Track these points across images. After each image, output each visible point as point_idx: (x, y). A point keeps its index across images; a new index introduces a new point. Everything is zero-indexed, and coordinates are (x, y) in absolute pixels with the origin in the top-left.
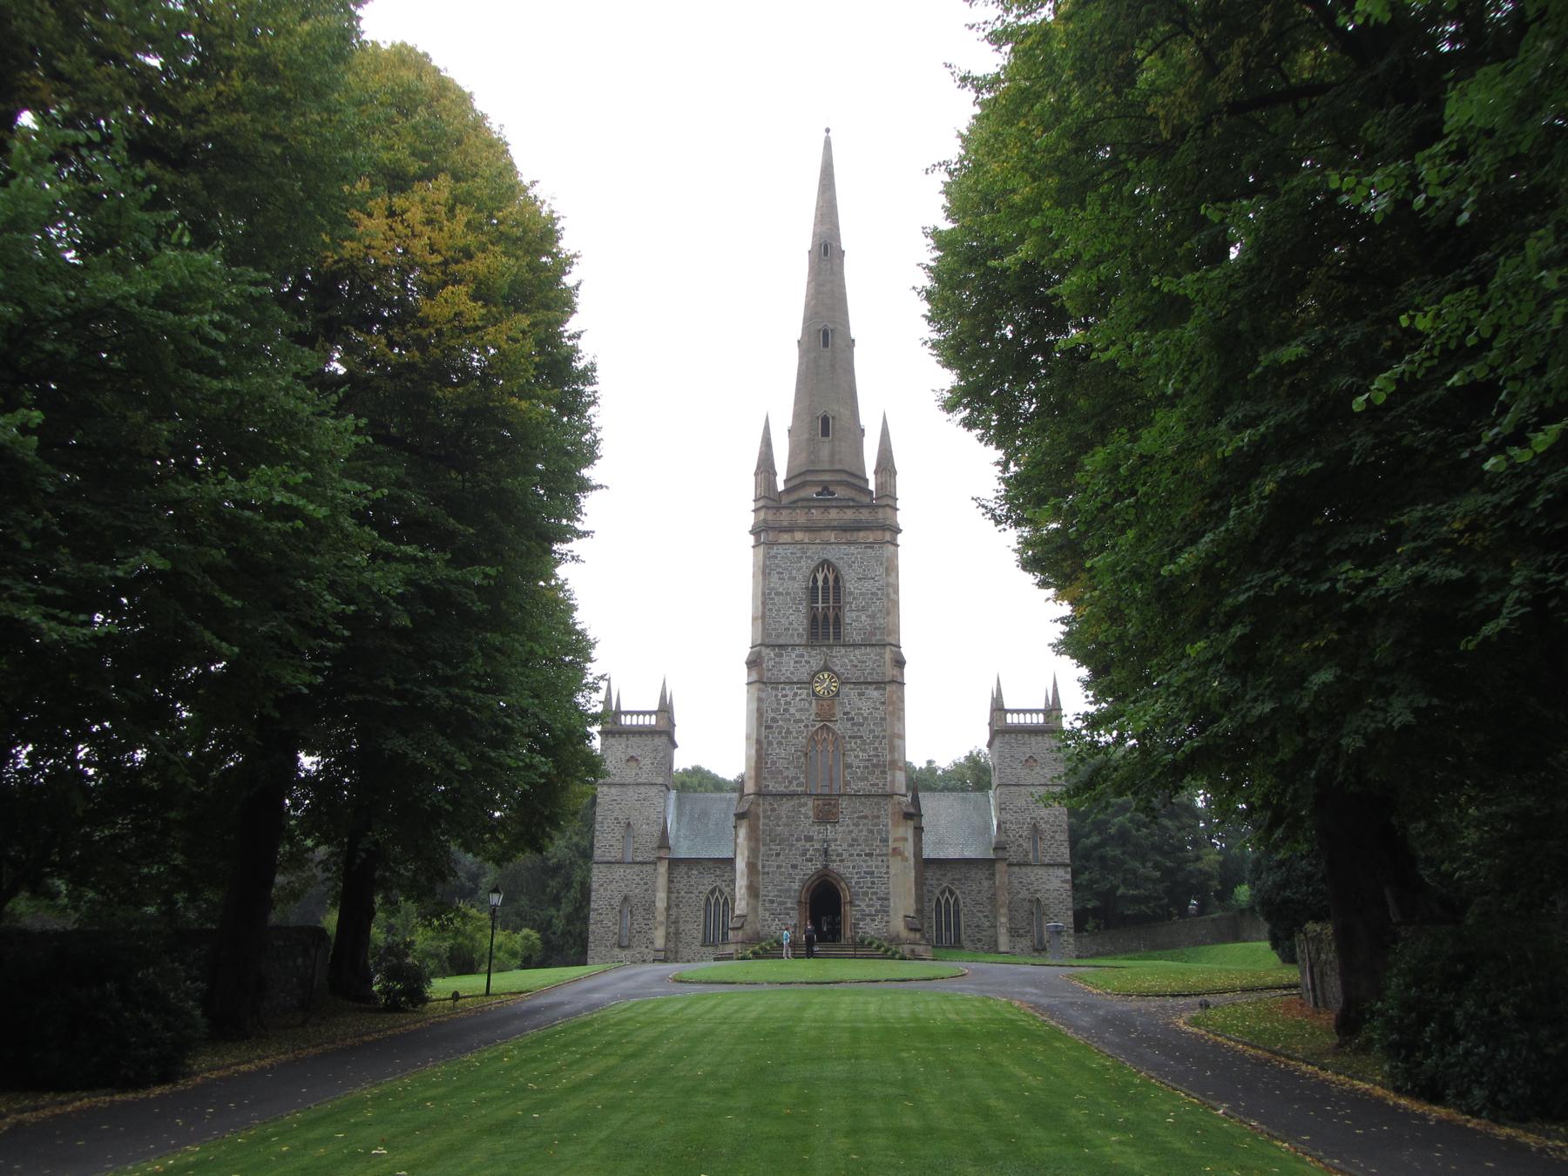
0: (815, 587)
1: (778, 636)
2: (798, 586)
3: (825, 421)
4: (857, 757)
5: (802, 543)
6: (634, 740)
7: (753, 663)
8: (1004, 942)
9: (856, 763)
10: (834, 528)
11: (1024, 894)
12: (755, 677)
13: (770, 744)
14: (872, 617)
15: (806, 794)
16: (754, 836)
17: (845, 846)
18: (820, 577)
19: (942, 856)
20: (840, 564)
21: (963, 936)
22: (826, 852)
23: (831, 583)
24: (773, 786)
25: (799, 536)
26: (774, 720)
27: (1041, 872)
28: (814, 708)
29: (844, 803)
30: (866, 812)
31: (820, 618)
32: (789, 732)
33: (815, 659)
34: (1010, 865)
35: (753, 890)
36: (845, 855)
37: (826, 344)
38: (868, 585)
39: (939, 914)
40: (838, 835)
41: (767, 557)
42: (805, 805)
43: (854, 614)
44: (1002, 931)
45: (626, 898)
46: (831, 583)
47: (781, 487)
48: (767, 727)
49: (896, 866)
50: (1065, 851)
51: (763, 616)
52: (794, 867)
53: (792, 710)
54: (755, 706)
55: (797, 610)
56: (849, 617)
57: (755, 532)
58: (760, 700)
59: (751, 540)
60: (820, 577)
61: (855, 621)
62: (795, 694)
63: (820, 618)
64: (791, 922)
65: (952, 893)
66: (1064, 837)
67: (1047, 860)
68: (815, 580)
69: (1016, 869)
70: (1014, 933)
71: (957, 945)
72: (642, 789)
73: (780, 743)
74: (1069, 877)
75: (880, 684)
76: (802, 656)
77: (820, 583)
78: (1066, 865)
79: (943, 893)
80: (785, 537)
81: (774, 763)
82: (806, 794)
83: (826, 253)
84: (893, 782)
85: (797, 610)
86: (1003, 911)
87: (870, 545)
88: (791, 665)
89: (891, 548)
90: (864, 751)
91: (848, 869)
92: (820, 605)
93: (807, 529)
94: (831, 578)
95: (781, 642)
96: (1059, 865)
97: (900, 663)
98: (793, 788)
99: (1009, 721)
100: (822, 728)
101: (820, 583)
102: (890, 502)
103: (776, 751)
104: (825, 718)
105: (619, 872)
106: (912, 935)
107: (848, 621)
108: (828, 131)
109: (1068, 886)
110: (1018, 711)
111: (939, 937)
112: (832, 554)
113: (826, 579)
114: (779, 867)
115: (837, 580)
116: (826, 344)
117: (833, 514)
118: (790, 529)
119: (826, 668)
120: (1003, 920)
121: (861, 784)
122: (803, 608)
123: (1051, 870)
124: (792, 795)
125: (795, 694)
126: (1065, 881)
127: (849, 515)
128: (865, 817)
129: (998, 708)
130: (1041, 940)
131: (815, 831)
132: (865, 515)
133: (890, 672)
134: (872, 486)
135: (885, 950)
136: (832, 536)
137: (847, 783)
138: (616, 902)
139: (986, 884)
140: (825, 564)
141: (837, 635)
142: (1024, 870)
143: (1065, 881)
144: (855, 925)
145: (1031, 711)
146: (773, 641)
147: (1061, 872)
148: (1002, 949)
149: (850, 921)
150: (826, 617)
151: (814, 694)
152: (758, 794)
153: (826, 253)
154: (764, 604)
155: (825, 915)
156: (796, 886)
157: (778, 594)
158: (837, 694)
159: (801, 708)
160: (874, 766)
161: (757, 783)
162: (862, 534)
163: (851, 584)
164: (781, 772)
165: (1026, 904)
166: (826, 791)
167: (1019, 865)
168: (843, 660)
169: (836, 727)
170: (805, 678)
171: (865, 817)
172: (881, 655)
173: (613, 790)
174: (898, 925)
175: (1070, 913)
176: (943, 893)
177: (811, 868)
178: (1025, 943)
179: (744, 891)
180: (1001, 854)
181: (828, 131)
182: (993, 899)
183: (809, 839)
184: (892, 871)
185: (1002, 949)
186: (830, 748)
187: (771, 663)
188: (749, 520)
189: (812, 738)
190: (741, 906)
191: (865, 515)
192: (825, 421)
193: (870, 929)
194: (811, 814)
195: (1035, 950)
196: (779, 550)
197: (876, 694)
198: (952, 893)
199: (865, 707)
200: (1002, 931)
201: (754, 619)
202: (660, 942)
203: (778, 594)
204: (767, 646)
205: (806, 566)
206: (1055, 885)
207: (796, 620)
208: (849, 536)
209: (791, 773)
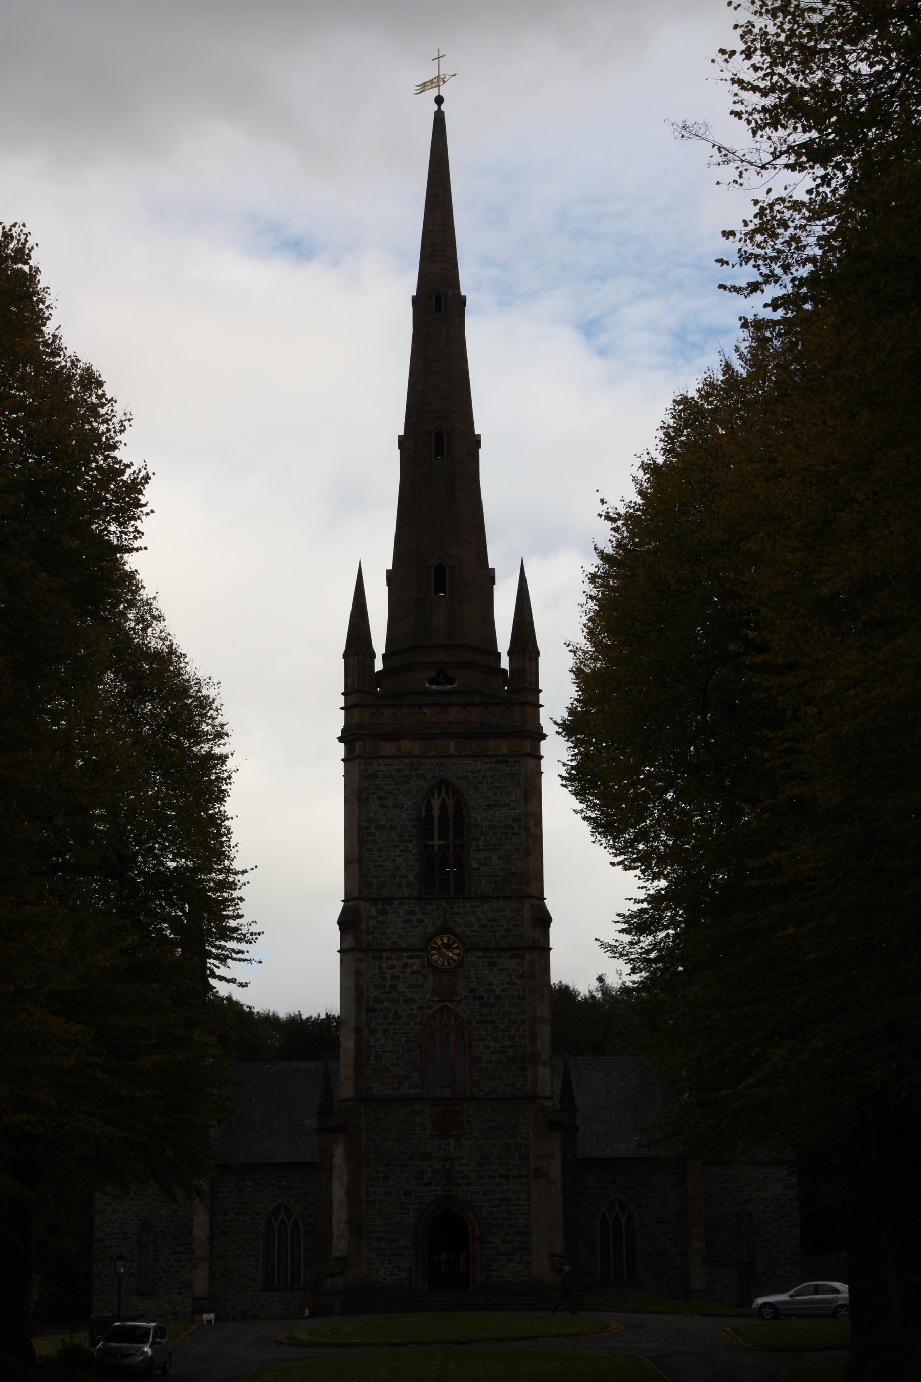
0: (429, 816)
3: (440, 570)
7: (346, 922)
18: (436, 804)
23: (451, 812)
25: (406, 745)
37: (439, 452)
46: (451, 812)
47: (378, 665)
53: (402, 987)
58: (358, 974)
60: (436, 804)
62: (405, 965)
77: (436, 812)
80: (389, 748)
83: (438, 308)
89: (531, 762)
94: (451, 803)
97: (544, 920)
101: (436, 812)
107: (474, 864)
108: (439, 100)
113: (443, 807)
116: (439, 452)
119: (446, 929)
125: (405, 965)
134: (505, 664)
151: (430, 965)
153: (438, 308)
154: (361, 842)
157: (379, 827)
158: (461, 965)
181: (439, 100)
187: (372, 923)
190: (340, 1246)
192: (440, 570)
202: (201, 1287)
203: (379, 827)
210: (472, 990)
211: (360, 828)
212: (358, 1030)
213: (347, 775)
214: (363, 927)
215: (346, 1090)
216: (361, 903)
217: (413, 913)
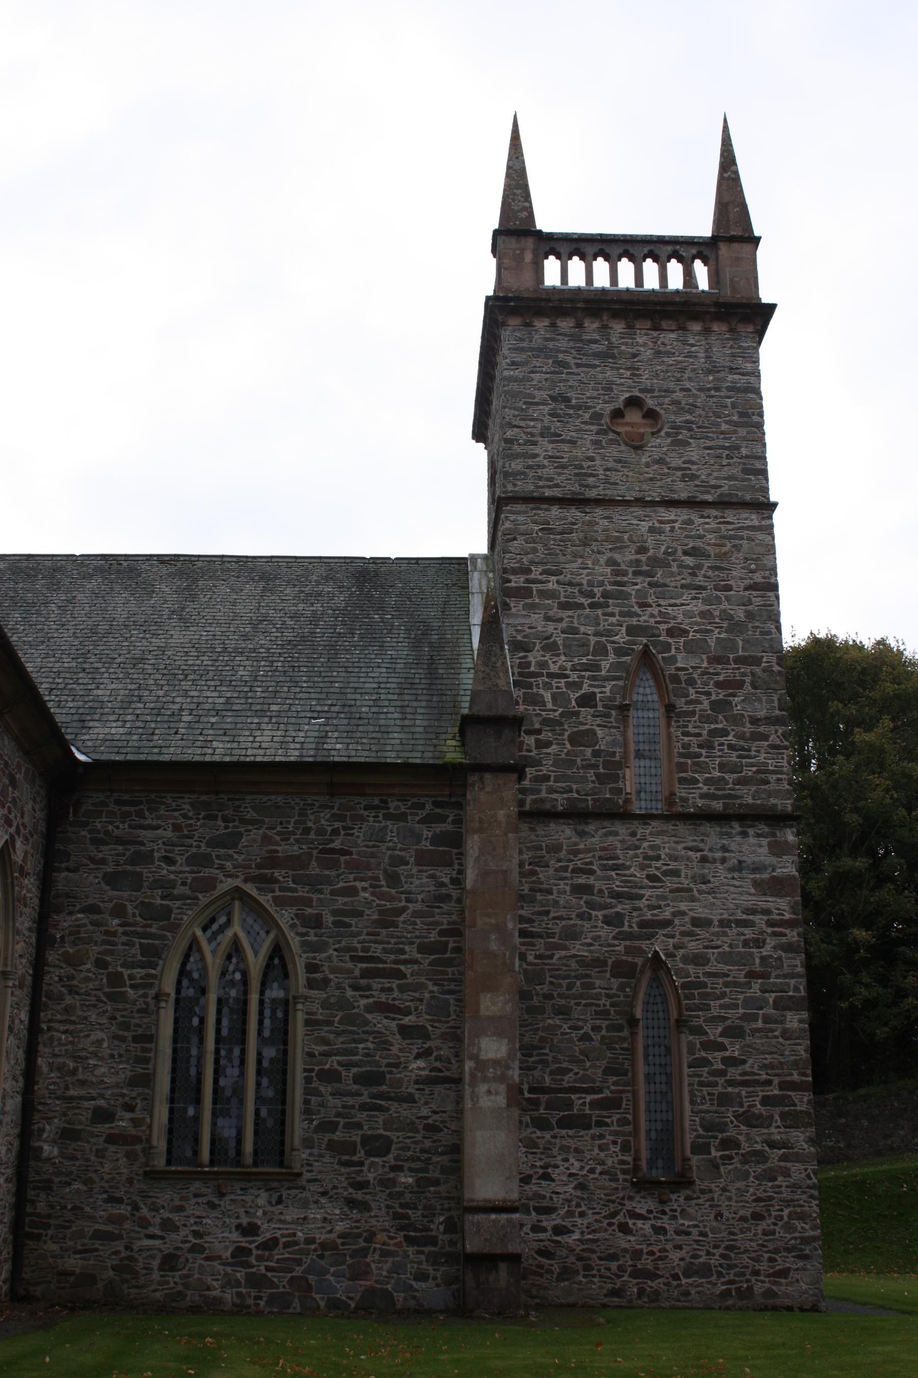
11: (597, 938)
19: (219, 751)
21: (298, 1127)
27: (669, 843)
44: (488, 1099)
67: (694, 798)
69: (564, 833)
74: (788, 867)
78: (776, 819)
86: (494, 1004)
96: (748, 818)
109: (783, 906)
111: (181, 1129)
120: (493, 1048)
123: (712, 836)
126: (776, 886)
129: (517, 234)
130: (666, 1139)
139: (419, 882)
142: (597, 836)
143: (776, 886)
147: (753, 847)
165: (604, 983)
167: (576, 815)
175: (795, 1020)
180: (492, 749)
182: (449, 951)
195: (643, 1185)
200: (488, 1099)
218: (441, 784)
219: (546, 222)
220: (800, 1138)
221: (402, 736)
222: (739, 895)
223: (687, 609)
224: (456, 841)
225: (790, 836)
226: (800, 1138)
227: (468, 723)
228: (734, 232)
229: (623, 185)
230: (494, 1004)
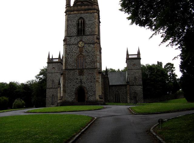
1: (70, 34)
2: (75, 23)
4: (88, 60)
5: (76, 14)
6: (54, 64)
7: (64, 41)
8: (129, 101)
9: (88, 61)
10: (83, 10)
12: (65, 43)
13: (68, 58)
14: (92, 29)
15: (76, 69)
16: (64, 79)
17: (85, 80)
18: (80, 21)
19: (116, 84)
20: (84, 18)
21: (120, 100)
22: (81, 81)
23: (82, 22)
24: (69, 67)
25: (75, 12)
26: (69, 53)
27: (136, 87)
28: (78, 50)
29: (85, 71)
30: (90, 72)
31: (80, 30)
32: (73, 55)
33: (79, 39)
34: (130, 86)
35: (64, 91)
36: (85, 82)
38: (91, 22)
39: (115, 96)
40: (84, 78)
41: (68, 17)
42: (76, 71)
43: (87, 29)
44: (128, 99)
45: (53, 95)
46: (82, 22)
48: (68, 54)
49: (97, 84)
50: (141, 82)
51: (67, 30)
52: (74, 85)
54: (65, 50)
55: (75, 28)
56: (86, 29)
57: (66, 12)
58: (66, 48)
59: (65, 14)
60: (80, 21)
61: (88, 30)
62: (74, 47)
63: (80, 30)
64: (73, 98)
65: (118, 92)
66: (141, 79)
68: (79, 22)
69: (131, 86)
70: (131, 99)
71: (119, 102)
72: (56, 74)
73: (71, 58)
74: (142, 87)
75: (93, 44)
76: (76, 38)
77: (80, 22)
79: (116, 92)
80: (72, 13)
81: (69, 62)
82: (76, 69)
84: (96, 65)
85: (75, 28)
86: (128, 95)
87: (91, 13)
88: (73, 40)
90: (90, 59)
91: (86, 85)
92: (80, 27)
93: (77, 11)
95: (71, 35)
98: (74, 68)
99: (130, 57)
100: (80, 54)
101: (80, 22)
102: (96, 4)
103: (70, 60)
104: (81, 52)
105: (51, 90)
106: (101, 100)
109: (142, 89)
110: (131, 55)
112: (83, 16)
113: (81, 21)
114: (70, 85)
115: (84, 21)
117: (83, 7)
118: (73, 11)
121: (89, 66)
122: (76, 28)
124: (74, 69)
126: (141, 88)
127: (86, 7)
128: (90, 73)
131: (78, 77)
132: (90, 7)
133: (96, 41)
135: (95, 103)
136: (83, 12)
137: (86, 66)
138: (51, 96)
139: (125, 90)
140: (81, 18)
141: (84, 33)
144: (88, 98)
145: (134, 55)
146: (69, 35)
147: (140, 87)
148: (128, 102)
149: (87, 97)
150: (81, 30)
152: (66, 69)
154: (67, 27)
155: (81, 97)
156: (74, 90)
158: (84, 46)
159: (75, 50)
160: (93, 62)
161: (65, 67)
162: (89, 11)
163: (87, 22)
164: (71, 64)
166: (81, 68)
167: (132, 85)
168: (85, 38)
169: (84, 54)
170: (76, 43)
171: (90, 73)
172: (94, 37)
173: (50, 74)
174: (98, 98)
176: (116, 92)
177: (78, 85)
178: (133, 101)
179: (62, 91)
180: (128, 84)
182: (126, 92)
183: (77, 79)
184: (96, 86)
185: (128, 102)
186: (82, 58)
187: (69, 40)
188: (65, 10)
189: (78, 57)
191: (90, 7)
193: (91, 99)
194: (78, 73)
196: (71, 16)
197: (92, 46)
198: (118, 92)
199: (90, 49)
201: (65, 31)
204: (68, 37)
205: (77, 18)
206: (139, 89)
207: (74, 30)
208: (86, 12)
209: (73, 64)
210: (86, 50)
211: (67, 25)
212: (66, 58)
213: (68, 20)
214: (67, 41)
215: (64, 68)
216: (67, 37)
217: (76, 38)
218: (125, 85)
219: (129, 54)
220: (143, 100)
221: (124, 83)
222: (140, 89)
223: (137, 75)
224: (126, 88)
225: (142, 86)
226: (143, 100)
227: (127, 82)
228: (139, 54)
229: (133, 52)
230: (128, 95)
